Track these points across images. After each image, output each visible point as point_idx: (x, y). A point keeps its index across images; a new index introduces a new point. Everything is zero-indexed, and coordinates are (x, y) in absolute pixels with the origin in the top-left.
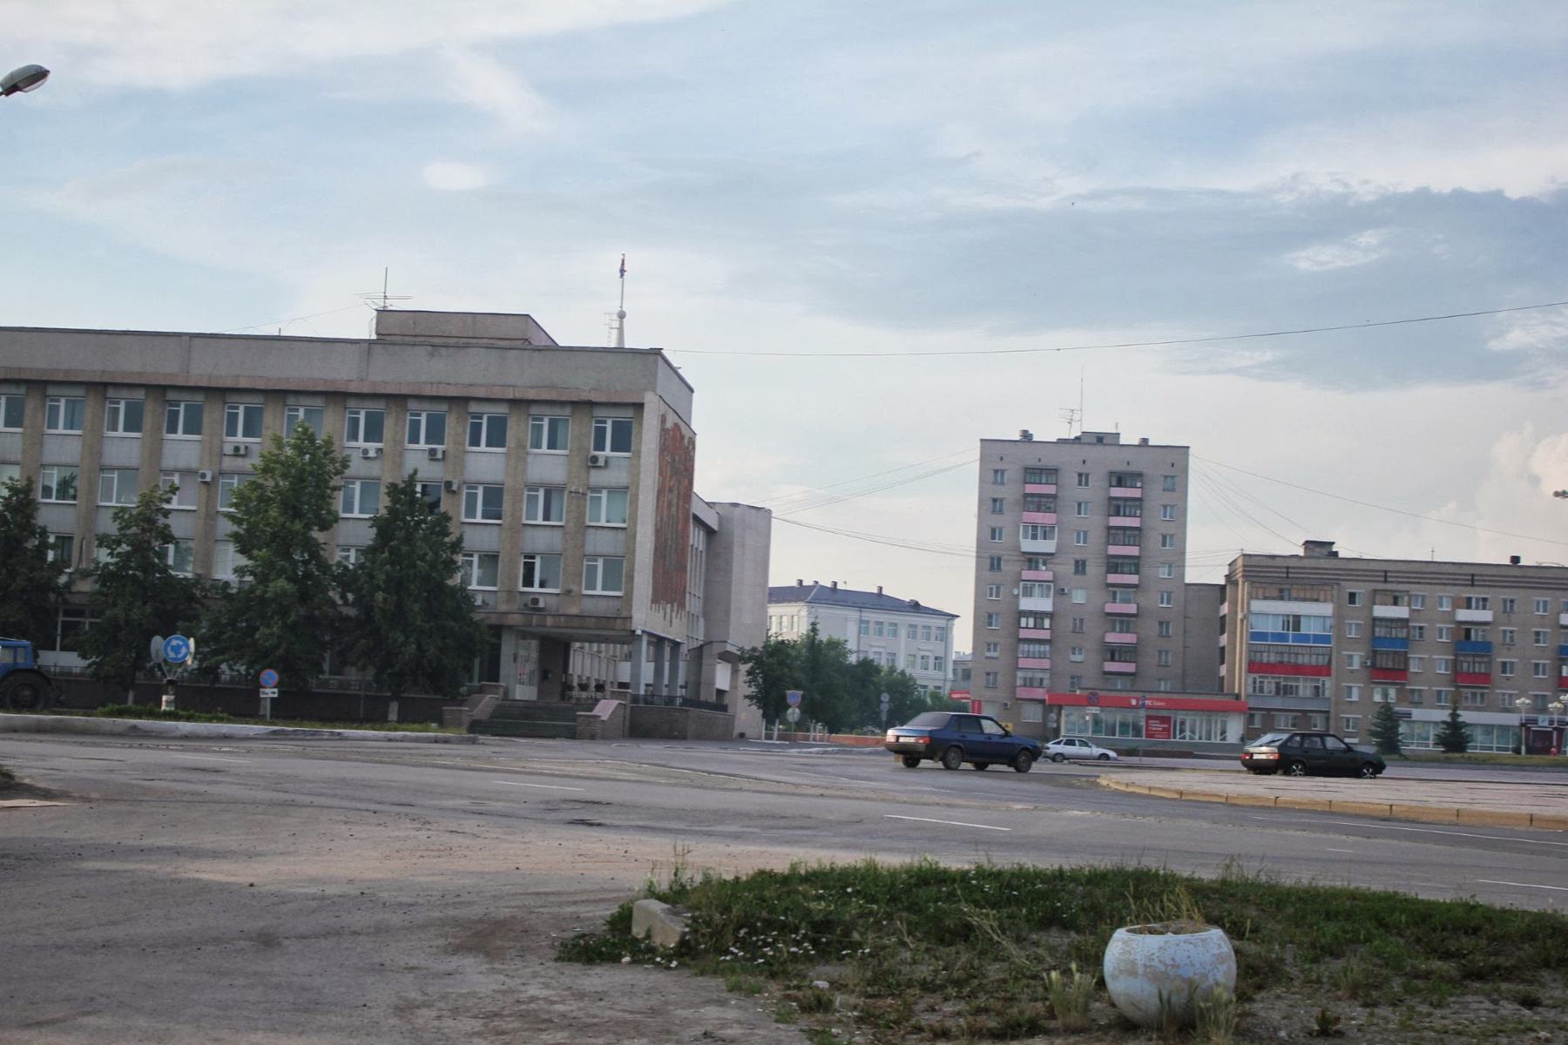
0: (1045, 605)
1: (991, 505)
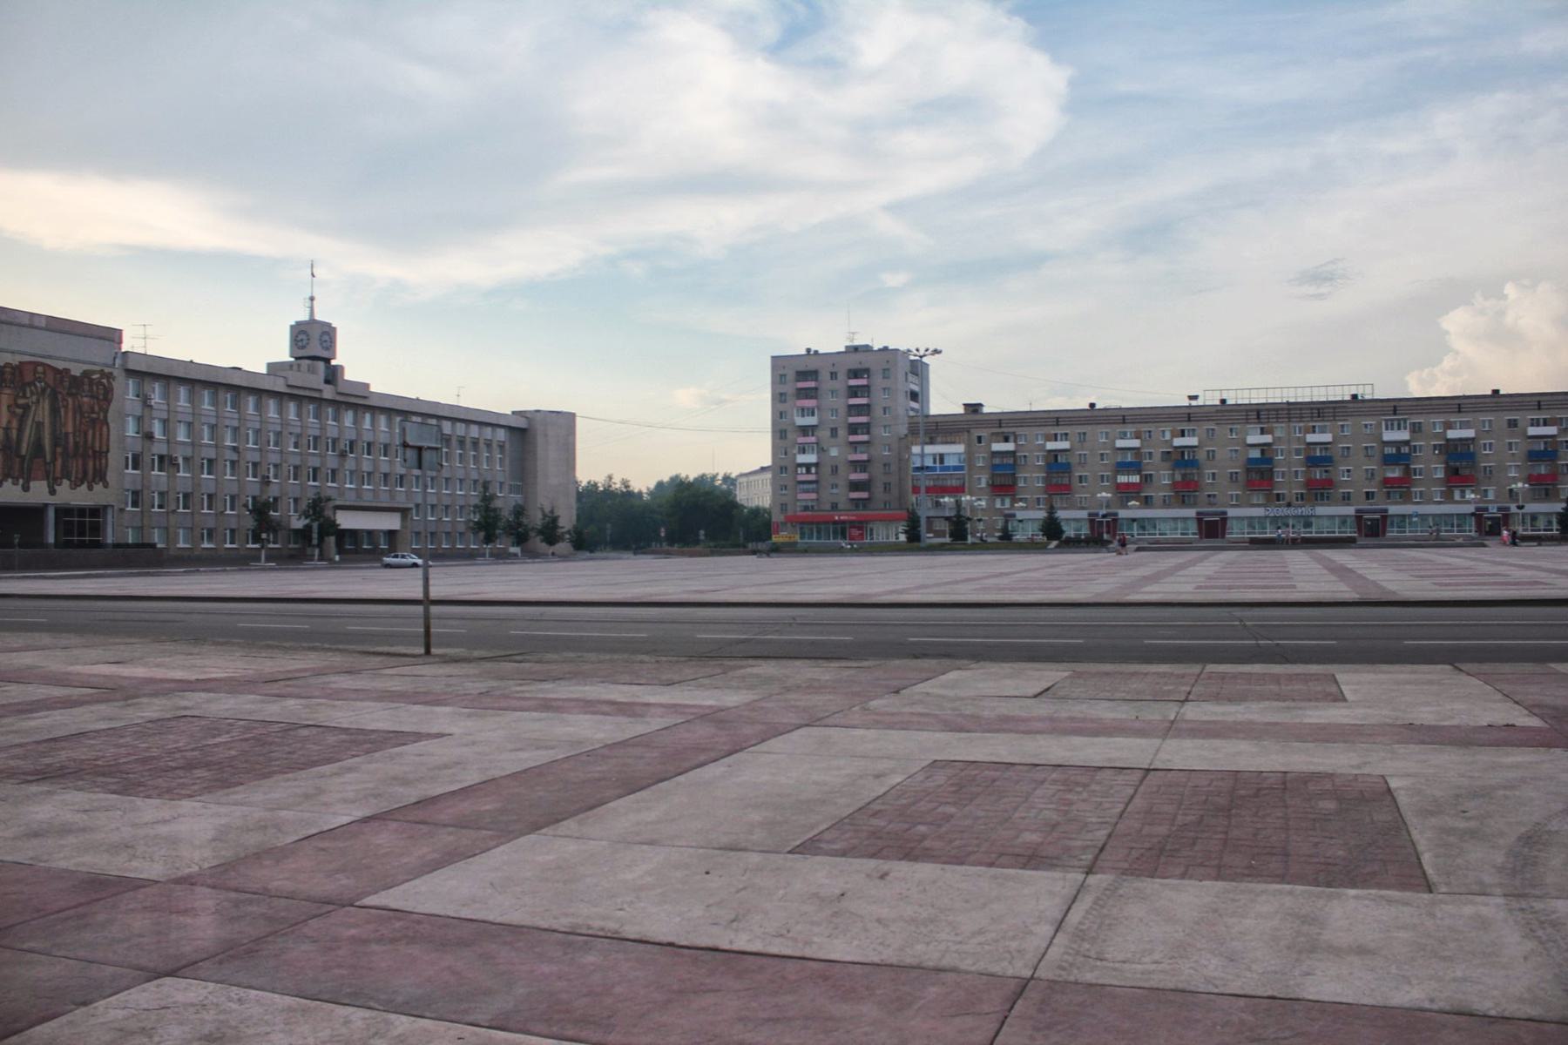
0: (811, 458)
1: (779, 398)
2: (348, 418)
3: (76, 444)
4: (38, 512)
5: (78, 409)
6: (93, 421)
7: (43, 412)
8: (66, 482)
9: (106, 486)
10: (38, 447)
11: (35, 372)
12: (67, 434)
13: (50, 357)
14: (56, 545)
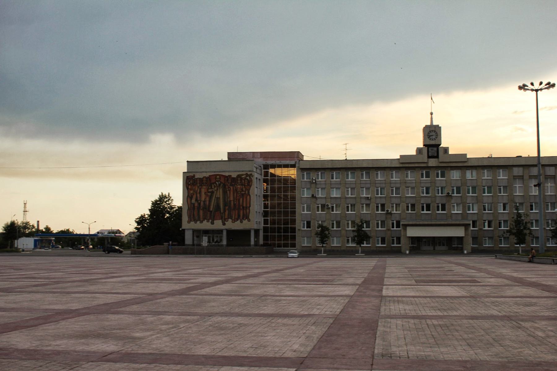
2: (455, 175)
3: (235, 205)
4: (220, 232)
5: (236, 190)
6: (243, 195)
7: (220, 193)
8: (230, 220)
9: (249, 220)
10: (218, 207)
11: (216, 178)
12: (230, 201)
13: (224, 171)
14: (228, 245)
